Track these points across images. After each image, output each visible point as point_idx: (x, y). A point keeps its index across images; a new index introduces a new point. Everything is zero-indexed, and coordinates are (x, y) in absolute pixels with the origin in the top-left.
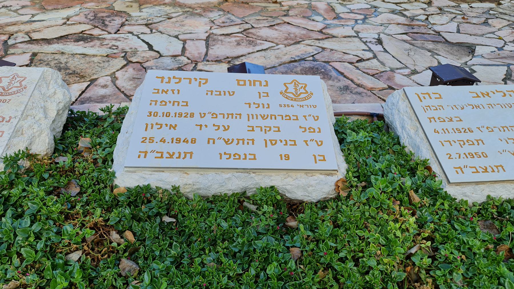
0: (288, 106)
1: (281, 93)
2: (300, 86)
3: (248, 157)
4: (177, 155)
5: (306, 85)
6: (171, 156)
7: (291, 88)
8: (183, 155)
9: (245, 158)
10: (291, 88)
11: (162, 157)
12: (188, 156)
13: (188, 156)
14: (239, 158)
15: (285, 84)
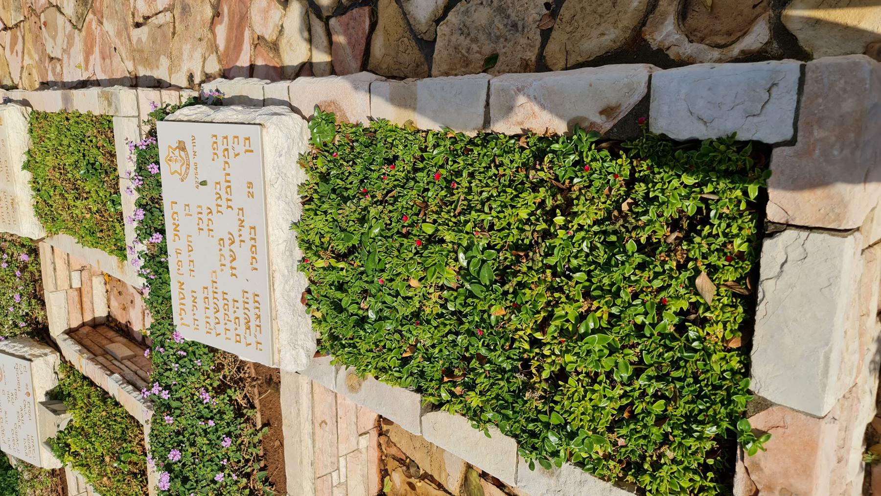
0: (196, 174)
1: (183, 181)
2: (171, 154)
3: (253, 236)
4: (257, 310)
5: (170, 147)
6: (259, 317)
7: (176, 166)
8: (257, 305)
9: (254, 239)
10: (176, 166)
11: (259, 326)
12: (257, 298)
13: (257, 298)
14: (255, 246)
15: (172, 174)
